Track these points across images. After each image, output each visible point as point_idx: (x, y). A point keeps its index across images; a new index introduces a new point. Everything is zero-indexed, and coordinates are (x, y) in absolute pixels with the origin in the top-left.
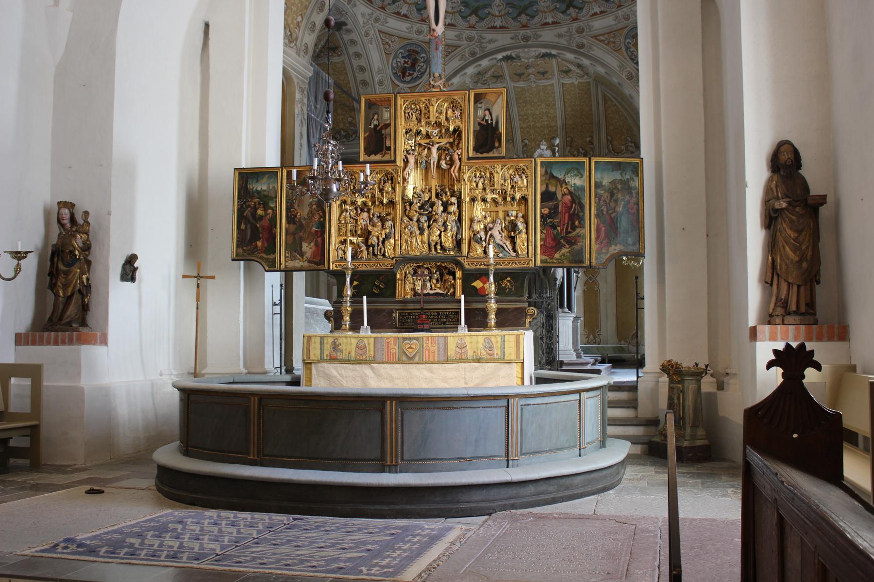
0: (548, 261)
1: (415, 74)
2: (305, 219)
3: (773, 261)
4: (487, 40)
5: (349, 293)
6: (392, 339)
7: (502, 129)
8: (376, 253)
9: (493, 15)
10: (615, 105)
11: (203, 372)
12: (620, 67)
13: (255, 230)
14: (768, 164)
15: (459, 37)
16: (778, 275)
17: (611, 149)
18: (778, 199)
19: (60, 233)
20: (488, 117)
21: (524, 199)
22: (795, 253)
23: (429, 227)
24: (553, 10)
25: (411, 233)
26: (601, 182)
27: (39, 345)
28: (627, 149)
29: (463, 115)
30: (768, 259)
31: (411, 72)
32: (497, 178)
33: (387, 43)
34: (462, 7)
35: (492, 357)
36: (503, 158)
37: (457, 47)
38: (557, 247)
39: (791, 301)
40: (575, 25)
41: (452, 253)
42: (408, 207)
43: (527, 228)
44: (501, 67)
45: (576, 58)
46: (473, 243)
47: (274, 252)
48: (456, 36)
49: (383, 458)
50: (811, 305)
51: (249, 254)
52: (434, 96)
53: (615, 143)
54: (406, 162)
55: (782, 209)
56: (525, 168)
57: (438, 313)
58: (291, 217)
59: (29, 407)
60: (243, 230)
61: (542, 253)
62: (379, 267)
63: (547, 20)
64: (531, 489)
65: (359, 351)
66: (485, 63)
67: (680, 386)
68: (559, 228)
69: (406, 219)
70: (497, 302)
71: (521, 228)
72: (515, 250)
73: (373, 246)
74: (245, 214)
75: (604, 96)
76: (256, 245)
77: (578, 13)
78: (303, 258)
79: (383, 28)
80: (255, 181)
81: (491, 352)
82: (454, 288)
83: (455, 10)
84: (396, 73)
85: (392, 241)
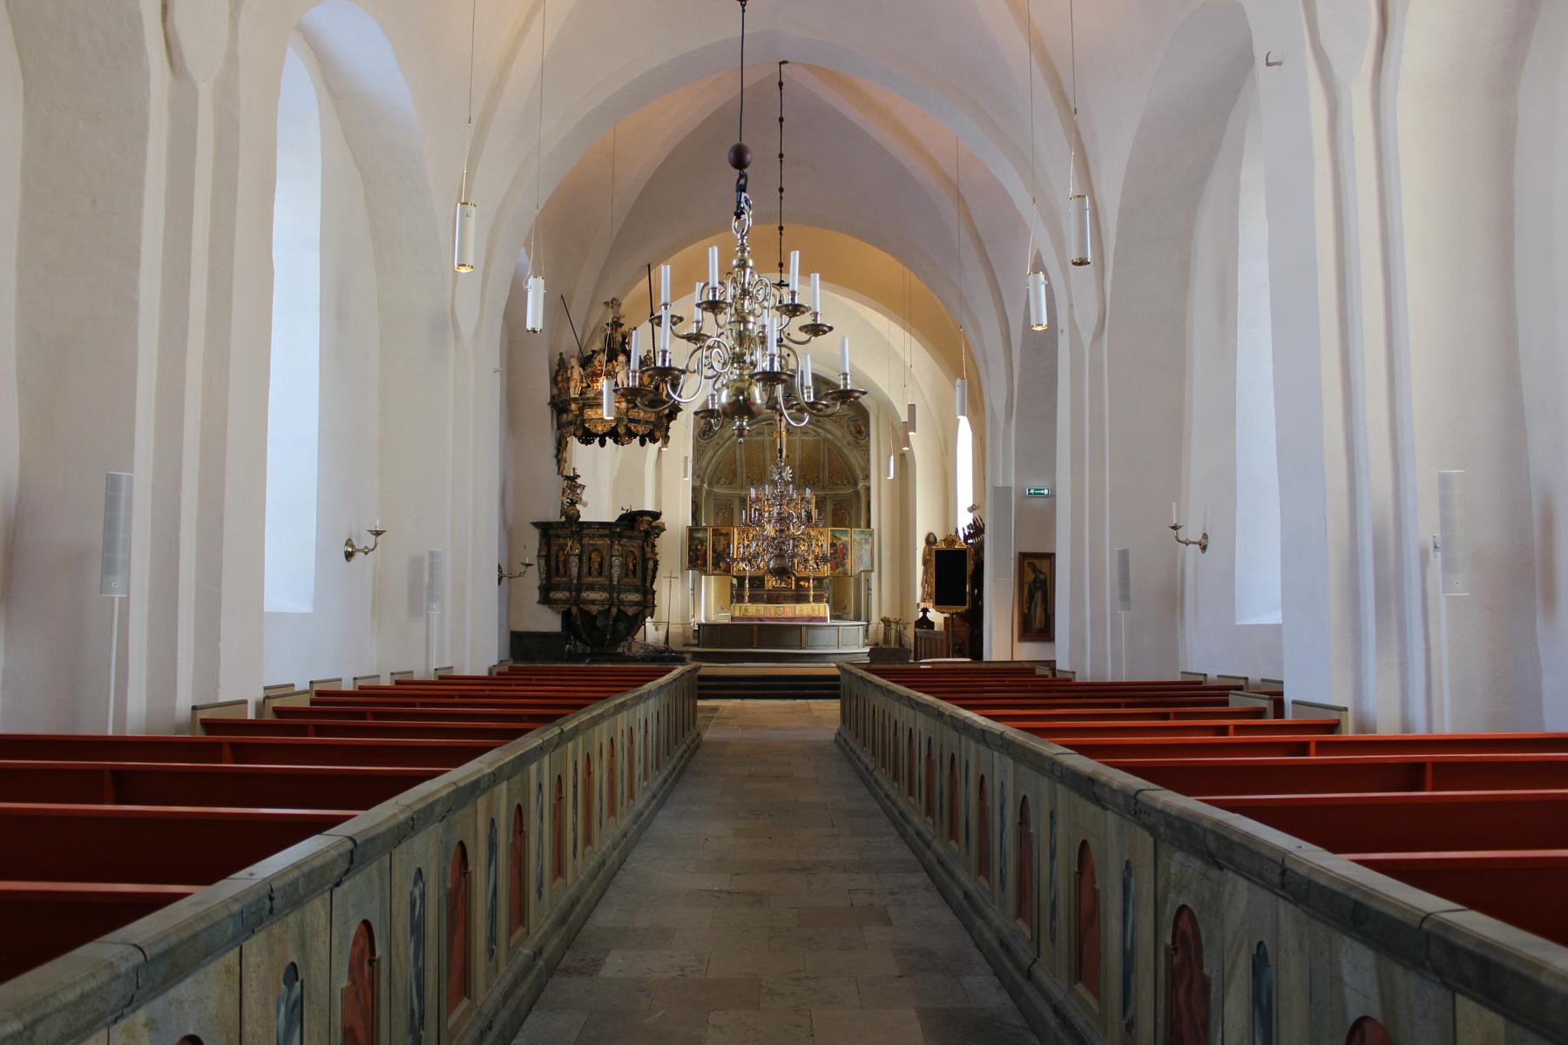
13: (697, 555)
28: (842, 482)
38: (837, 567)
53: (834, 478)
61: (831, 570)
75: (829, 450)
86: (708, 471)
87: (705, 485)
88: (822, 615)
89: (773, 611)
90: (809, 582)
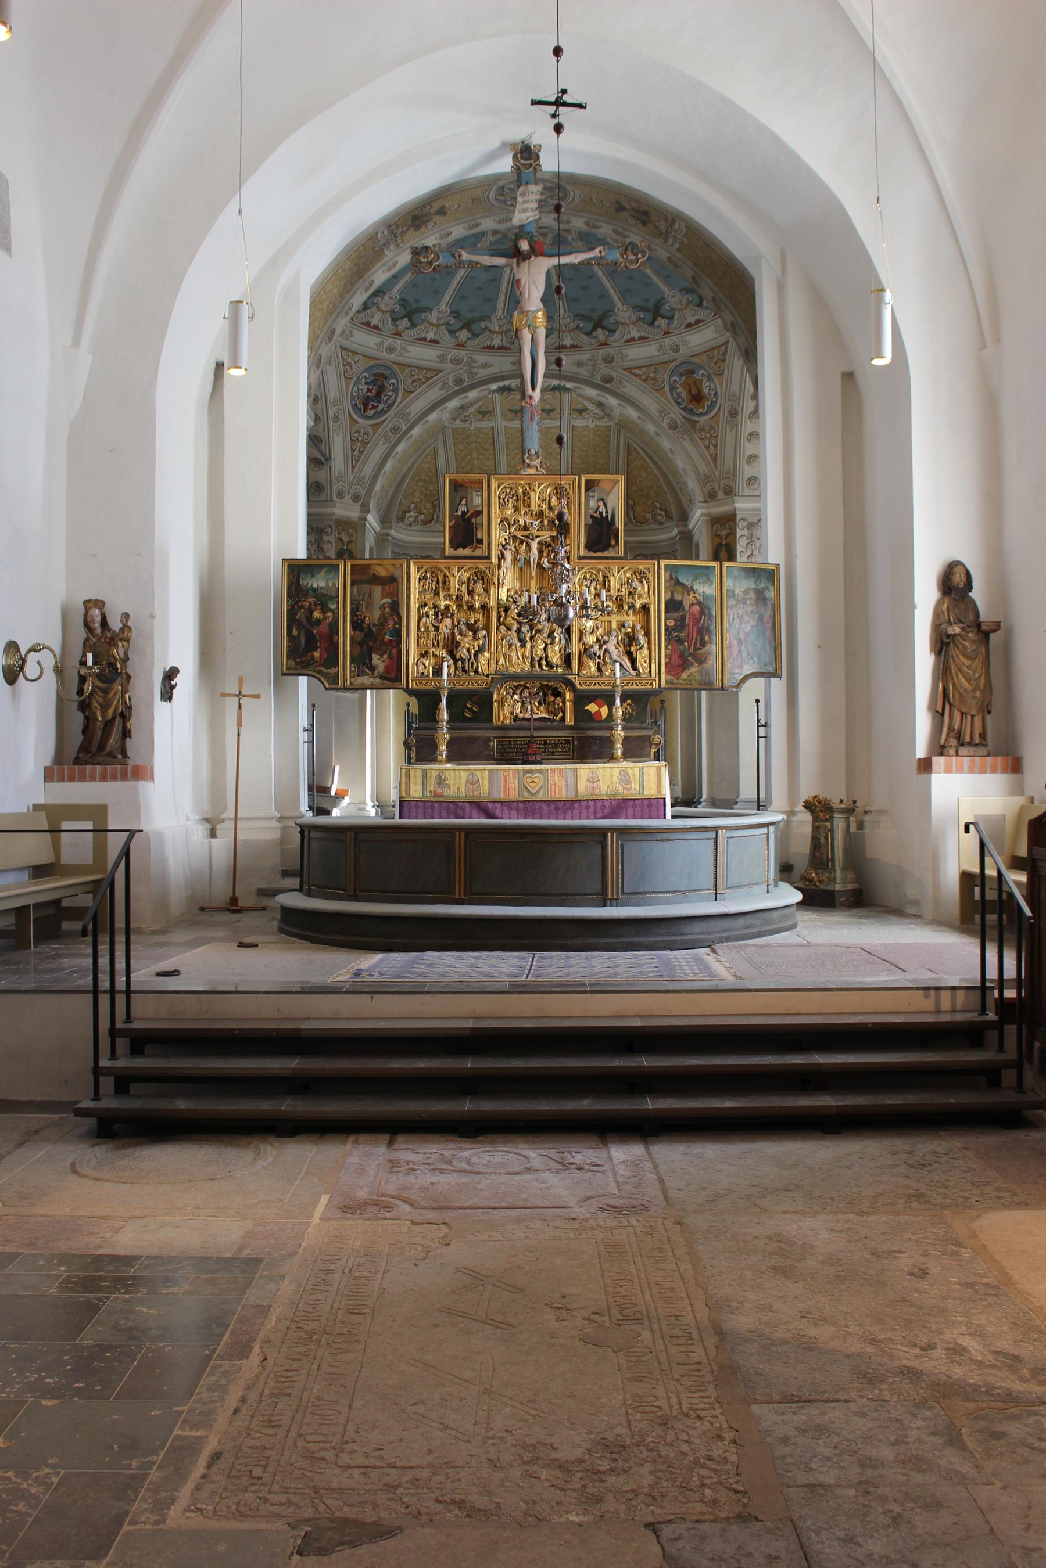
0: (675, 681)
1: (381, 407)
2: (375, 625)
3: (945, 690)
4: (480, 363)
5: (446, 717)
6: (511, 772)
7: (620, 524)
8: (467, 668)
9: (491, 331)
10: (643, 459)
11: (222, 816)
12: (660, 412)
14: (938, 586)
15: (442, 358)
16: (950, 704)
17: (632, 517)
18: (950, 623)
19: (87, 640)
20: (602, 509)
21: (645, 608)
22: (969, 682)
23: (532, 638)
24: (574, 330)
25: (510, 646)
26: (733, 591)
27: (79, 781)
29: (572, 505)
30: (938, 686)
31: (375, 404)
32: (614, 582)
33: (348, 363)
34: (451, 318)
35: (629, 792)
36: (621, 558)
37: (438, 371)
38: (684, 665)
39: (965, 732)
40: (602, 352)
41: (560, 670)
42: (503, 614)
43: (649, 643)
44: (493, 401)
45: (599, 395)
46: (585, 659)
47: (336, 665)
48: (437, 356)
49: (604, 892)
50: (983, 736)
51: (303, 668)
52: (536, 480)
53: (638, 509)
54: (502, 557)
55: (955, 635)
56: (646, 571)
57: (545, 741)
59: (91, 857)
60: (295, 637)
61: (668, 672)
62: (470, 686)
63: (564, 343)
64: (741, 922)
65: (470, 786)
66: (473, 394)
67: (829, 824)
68: (686, 644)
69: (503, 628)
70: (624, 729)
71: (642, 642)
72: (635, 668)
73: (463, 660)
74: (297, 617)
75: (628, 446)
76: (313, 656)
77: (608, 336)
78: (373, 674)
79: (347, 344)
80: (309, 576)
81: (629, 787)
82: (564, 713)
83: (441, 322)
84: (356, 405)
85: (486, 654)
86: (378, 487)
87: (372, 519)
88: (650, 792)
89: (514, 784)
90: (611, 705)
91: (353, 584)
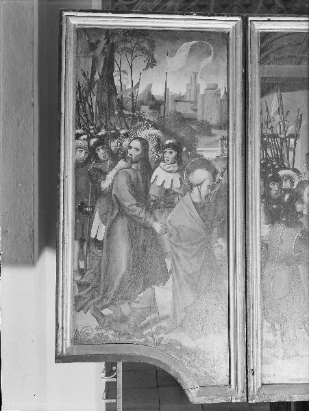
58: (279, 201)
91: (266, 89)
